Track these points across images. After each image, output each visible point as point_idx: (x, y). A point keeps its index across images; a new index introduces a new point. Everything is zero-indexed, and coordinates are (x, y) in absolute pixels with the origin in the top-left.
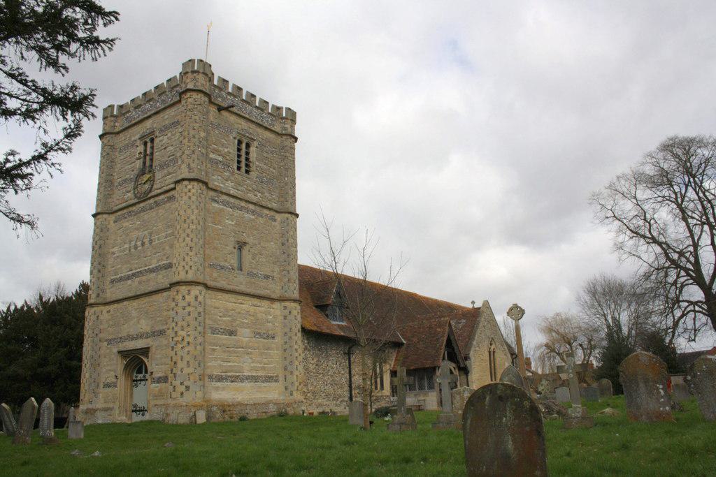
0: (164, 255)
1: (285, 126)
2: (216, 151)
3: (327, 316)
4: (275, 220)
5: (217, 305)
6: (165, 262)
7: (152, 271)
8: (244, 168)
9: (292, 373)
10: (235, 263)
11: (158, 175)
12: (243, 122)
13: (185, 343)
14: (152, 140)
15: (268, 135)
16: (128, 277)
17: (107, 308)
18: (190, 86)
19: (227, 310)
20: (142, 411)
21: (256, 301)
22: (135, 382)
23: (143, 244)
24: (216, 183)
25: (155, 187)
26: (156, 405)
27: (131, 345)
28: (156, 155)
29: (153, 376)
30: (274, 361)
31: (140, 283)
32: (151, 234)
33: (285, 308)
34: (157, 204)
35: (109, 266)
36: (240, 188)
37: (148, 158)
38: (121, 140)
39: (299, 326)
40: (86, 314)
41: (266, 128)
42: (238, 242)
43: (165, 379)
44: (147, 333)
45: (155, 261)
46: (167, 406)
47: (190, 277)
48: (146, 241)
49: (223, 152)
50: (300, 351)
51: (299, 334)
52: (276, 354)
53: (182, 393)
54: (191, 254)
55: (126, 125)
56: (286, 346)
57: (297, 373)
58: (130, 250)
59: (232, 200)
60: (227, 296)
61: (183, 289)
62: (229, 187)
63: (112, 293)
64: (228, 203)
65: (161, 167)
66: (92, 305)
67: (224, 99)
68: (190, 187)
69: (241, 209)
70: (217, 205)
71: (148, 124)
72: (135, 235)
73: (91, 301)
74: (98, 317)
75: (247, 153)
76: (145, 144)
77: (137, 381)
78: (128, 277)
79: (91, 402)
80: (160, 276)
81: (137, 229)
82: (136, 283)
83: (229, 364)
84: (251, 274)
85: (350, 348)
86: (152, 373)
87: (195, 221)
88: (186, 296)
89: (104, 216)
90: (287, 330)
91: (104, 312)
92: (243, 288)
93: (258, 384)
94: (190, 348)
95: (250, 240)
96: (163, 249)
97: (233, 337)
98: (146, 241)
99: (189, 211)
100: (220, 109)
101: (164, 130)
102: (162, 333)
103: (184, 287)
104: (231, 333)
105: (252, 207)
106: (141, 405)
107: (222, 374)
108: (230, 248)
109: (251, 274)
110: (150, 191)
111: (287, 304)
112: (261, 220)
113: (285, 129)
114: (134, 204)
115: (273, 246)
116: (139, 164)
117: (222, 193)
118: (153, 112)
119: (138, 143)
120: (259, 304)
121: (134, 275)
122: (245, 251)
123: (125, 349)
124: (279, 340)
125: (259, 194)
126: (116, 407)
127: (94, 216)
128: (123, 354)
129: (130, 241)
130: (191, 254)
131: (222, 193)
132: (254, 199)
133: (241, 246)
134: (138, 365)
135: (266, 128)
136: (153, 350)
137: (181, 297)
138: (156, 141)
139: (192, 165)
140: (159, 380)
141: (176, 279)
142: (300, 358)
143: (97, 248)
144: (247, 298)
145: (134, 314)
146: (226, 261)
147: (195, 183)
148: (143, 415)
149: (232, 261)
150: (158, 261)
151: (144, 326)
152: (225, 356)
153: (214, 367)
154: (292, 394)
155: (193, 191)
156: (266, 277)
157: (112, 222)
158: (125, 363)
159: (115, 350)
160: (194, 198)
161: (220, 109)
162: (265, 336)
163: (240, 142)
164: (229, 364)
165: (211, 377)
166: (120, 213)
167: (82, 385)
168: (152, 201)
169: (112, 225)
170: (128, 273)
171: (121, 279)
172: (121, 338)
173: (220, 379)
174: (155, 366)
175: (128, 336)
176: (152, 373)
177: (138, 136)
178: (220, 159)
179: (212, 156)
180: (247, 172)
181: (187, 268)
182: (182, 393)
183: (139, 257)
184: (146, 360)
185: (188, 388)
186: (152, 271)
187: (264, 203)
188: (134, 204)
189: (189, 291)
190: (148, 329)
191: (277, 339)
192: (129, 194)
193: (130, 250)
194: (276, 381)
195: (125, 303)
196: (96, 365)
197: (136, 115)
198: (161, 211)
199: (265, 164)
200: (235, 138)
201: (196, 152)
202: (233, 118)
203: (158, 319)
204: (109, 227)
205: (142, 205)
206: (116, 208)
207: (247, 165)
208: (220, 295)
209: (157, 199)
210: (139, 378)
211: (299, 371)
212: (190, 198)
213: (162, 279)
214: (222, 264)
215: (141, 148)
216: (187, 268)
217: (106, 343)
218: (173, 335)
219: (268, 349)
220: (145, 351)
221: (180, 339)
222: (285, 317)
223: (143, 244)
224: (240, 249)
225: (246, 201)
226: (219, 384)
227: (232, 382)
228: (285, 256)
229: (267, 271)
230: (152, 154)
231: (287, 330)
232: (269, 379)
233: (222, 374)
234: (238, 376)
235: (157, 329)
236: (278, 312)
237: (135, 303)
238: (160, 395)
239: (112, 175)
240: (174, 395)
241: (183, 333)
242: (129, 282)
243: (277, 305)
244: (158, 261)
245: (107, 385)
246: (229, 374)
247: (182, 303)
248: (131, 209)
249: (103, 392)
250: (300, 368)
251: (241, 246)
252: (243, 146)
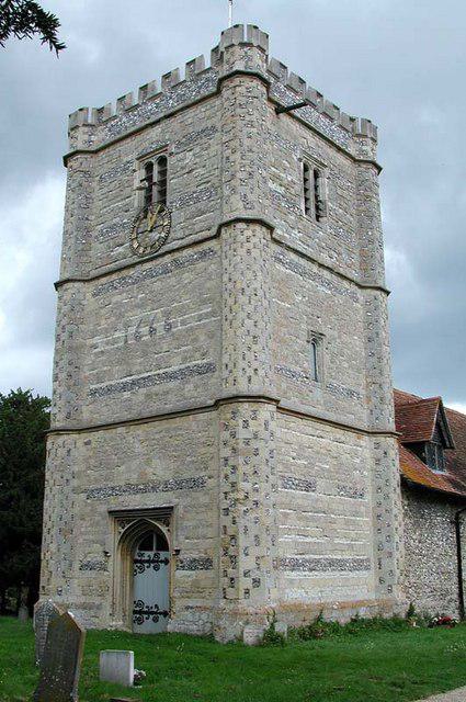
0: (196, 350)
1: (364, 148)
2: (275, 178)
3: (424, 460)
6: (199, 362)
7: (170, 377)
9: (390, 555)
11: (179, 216)
12: (308, 134)
13: (250, 504)
14: (162, 161)
16: (124, 387)
17: (85, 437)
18: (239, 66)
19: (301, 447)
20: (152, 613)
21: (339, 433)
22: (138, 565)
23: (152, 331)
25: (172, 235)
26: (187, 608)
27: (135, 502)
28: (172, 183)
29: (181, 557)
30: (359, 537)
31: (148, 396)
32: (167, 314)
33: (377, 445)
34: (177, 264)
35: (86, 368)
36: (310, 242)
37: (155, 189)
38: (102, 164)
39: (398, 477)
40: (49, 446)
41: (339, 149)
43: (207, 564)
44: (166, 483)
45: (178, 359)
46: (220, 613)
47: (255, 389)
48: (159, 326)
49: (286, 182)
50: (400, 517)
51: (398, 490)
52: (366, 521)
53: (247, 592)
54: (254, 347)
55: (109, 139)
56: (378, 511)
57: (397, 555)
58: (126, 342)
59: (303, 262)
61: (245, 409)
62: (294, 238)
63: (87, 415)
64: (296, 265)
65: (184, 203)
66: (58, 432)
68: (249, 233)
69: (314, 277)
70: (283, 269)
71: (155, 133)
72: (135, 316)
73: (55, 425)
74: (69, 451)
75: (316, 187)
76: (149, 167)
77: (141, 562)
78: (124, 387)
79: (59, 593)
80: (190, 387)
81: (138, 306)
82: (142, 398)
83: (307, 540)
84: (332, 389)
85: (457, 514)
86: (178, 551)
87: (260, 293)
88: (251, 422)
89: (76, 285)
90: (381, 482)
91: (80, 444)
92: (319, 411)
93: (343, 573)
94: (260, 512)
96: (195, 340)
97: (311, 493)
98: (159, 326)
99: (249, 275)
100: (279, 110)
101: (188, 142)
102: (196, 484)
103: (246, 405)
104: (309, 487)
105: (326, 273)
106: (149, 602)
107: (298, 557)
108: (302, 342)
109: (332, 389)
110: (165, 241)
111: (381, 439)
112: (339, 299)
113: (362, 152)
114: (133, 265)
115: (357, 342)
116: (137, 199)
117: (289, 248)
118: (162, 115)
119: (136, 165)
120: (343, 439)
121: (133, 383)
122: (323, 344)
123: (146, 507)
124: (368, 498)
126: (107, 604)
127: (58, 285)
128: (119, 516)
129: (127, 326)
130: (254, 347)
131: (289, 248)
132: (328, 262)
133: (316, 339)
134: (140, 538)
135: (339, 149)
136: (179, 512)
137: (241, 422)
138: (171, 161)
139: (251, 197)
140: (193, 565)
141: (229, 391)
142: (401, 530)
143: (64, 336)
144: (328, 428)
145: (139, 448)
147: (257, 228)
148: (155, 620)
149: (306, 365)
150: (185, 360)
151: (160, 470)
153: (287, 545)
154: (390, 591)
155: (254, 240)
156: (351, 393)
157: (89, 295)
158: (123, 531)
159: (103, 508)
160: (255, 253)
161: (279, 110)
162: (352, 492)
164: (307, 540)
166: (104, 280)
167: (43, 564)
168: (168, 258)
169: (90, 302)
170: (124, 380)
171: (109, 390)
172: (113, 488)
173: (295, 566)
174: (179, 538)
175: (129, 485)
176: (178, 551)
177: (135, 155)
178: (281, 190)
180: (318, 217)
181: (250, 372)
182: (247, 592)
183: (145, 354)
184: (164, 529)
185: (257, 582)
186: (170, 377)
188: (133, 265)
189: (254, 412)
190: (169, 476)
191: (368, 498)
192: (121, 249)
193: (126, 342)
194: (367, 568)
195: (121, 430)
196: (67, 531)
197: (129, 123)
198: (187, 277)
199: (340, 206)
200: (300, 160)
201: (257, 176)
202: (296, 127)
203: (189, 459)
204: (85, 302)
205: (147, 266)
206: (94, 273)
207: (317, 208)
208: (295, 422)
209: (177, 255)
210: (146, 558)
211: (399, 555)
212: (249, 251)
213: (194, 392)
214: (293, 368)
215: (142, 174)
216: (250, 372)
217: (83, 496)
218: (228, 489)
219: (356, 514)
220: (165, 514)
221: (241, 496)
222: (378, 462)
223: (152, 331)
224: (315, 343)
226: (293, 575)
227: (311, 570)
228: (374, 359)
230: (163, 183)
231: (381, 482)
232: (359, 565)
233: (298, 557)
234: (318, 561)
235: (186, 476)
236: (367, 454)
237: (141, 430)
238: (196, 589)
239: (87, 219)
240: (231, 592)
241: (247, 486)
242: (127, 395)
243: (366, 441)
244: (185, 360)
245: (85, 567)
246: (307, 557)
247: (243, 434)
248: (125, 273)
249: (79, 578)
250: (401, 546)
251: (316, 339)
252: (312, 173)
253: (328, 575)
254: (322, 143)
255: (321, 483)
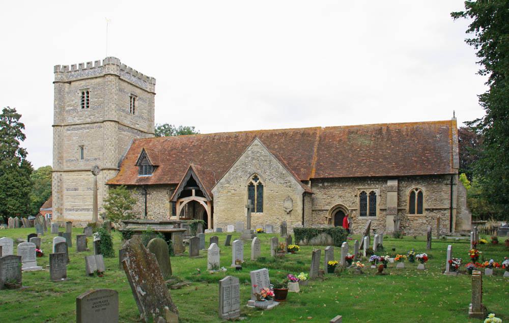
4: (102, 127)
5: (69, 178)
8: (85, 105)
10: (79, 156)
15: (98, 80)
24: (69, 121)
36: (81, 118)
42: (80, 146)
59: (77, 126)
60: (73, 173)
67: (73, 76)
69: (81, 129)
92: (83, 168)
95: (86, 143)
100: (70, 83)
104: (76, 190)
105: (87, 125)
112: (93, 130)
125: (92, 117)
133: (82, 148)
146: (74, 157)
152: (73, 200)
156: (96, 159)
163: (83, 93)
165: (66, 209)
173: (70, 210)
178: (72, 108)
179: (67, 109)
187: (95, 121)
214: (73, 159)
225: (84, 124)
229: (96, 156)
251: (82, 148)
253: (83, 212)
254: (89, 80)
255: (80, 188)
